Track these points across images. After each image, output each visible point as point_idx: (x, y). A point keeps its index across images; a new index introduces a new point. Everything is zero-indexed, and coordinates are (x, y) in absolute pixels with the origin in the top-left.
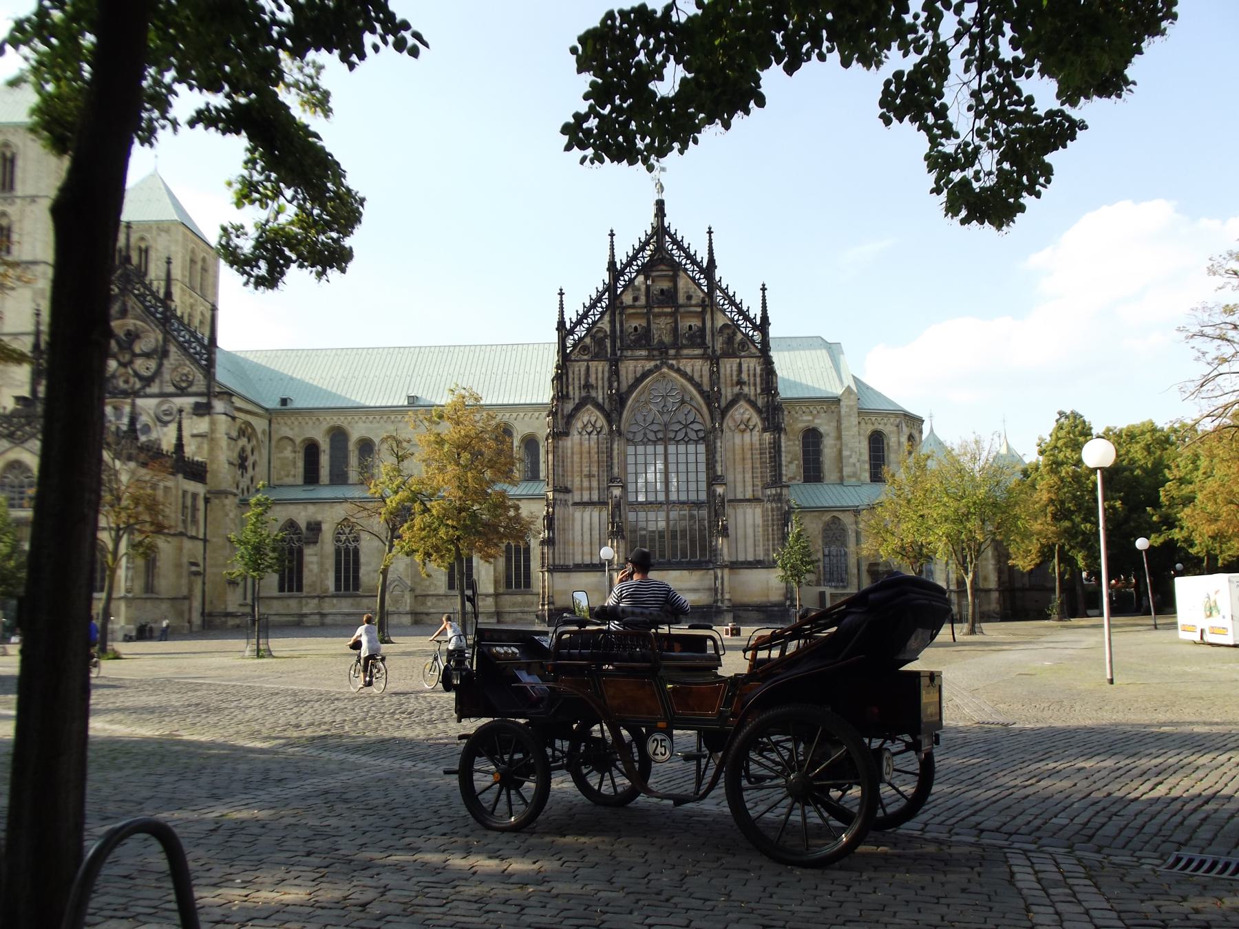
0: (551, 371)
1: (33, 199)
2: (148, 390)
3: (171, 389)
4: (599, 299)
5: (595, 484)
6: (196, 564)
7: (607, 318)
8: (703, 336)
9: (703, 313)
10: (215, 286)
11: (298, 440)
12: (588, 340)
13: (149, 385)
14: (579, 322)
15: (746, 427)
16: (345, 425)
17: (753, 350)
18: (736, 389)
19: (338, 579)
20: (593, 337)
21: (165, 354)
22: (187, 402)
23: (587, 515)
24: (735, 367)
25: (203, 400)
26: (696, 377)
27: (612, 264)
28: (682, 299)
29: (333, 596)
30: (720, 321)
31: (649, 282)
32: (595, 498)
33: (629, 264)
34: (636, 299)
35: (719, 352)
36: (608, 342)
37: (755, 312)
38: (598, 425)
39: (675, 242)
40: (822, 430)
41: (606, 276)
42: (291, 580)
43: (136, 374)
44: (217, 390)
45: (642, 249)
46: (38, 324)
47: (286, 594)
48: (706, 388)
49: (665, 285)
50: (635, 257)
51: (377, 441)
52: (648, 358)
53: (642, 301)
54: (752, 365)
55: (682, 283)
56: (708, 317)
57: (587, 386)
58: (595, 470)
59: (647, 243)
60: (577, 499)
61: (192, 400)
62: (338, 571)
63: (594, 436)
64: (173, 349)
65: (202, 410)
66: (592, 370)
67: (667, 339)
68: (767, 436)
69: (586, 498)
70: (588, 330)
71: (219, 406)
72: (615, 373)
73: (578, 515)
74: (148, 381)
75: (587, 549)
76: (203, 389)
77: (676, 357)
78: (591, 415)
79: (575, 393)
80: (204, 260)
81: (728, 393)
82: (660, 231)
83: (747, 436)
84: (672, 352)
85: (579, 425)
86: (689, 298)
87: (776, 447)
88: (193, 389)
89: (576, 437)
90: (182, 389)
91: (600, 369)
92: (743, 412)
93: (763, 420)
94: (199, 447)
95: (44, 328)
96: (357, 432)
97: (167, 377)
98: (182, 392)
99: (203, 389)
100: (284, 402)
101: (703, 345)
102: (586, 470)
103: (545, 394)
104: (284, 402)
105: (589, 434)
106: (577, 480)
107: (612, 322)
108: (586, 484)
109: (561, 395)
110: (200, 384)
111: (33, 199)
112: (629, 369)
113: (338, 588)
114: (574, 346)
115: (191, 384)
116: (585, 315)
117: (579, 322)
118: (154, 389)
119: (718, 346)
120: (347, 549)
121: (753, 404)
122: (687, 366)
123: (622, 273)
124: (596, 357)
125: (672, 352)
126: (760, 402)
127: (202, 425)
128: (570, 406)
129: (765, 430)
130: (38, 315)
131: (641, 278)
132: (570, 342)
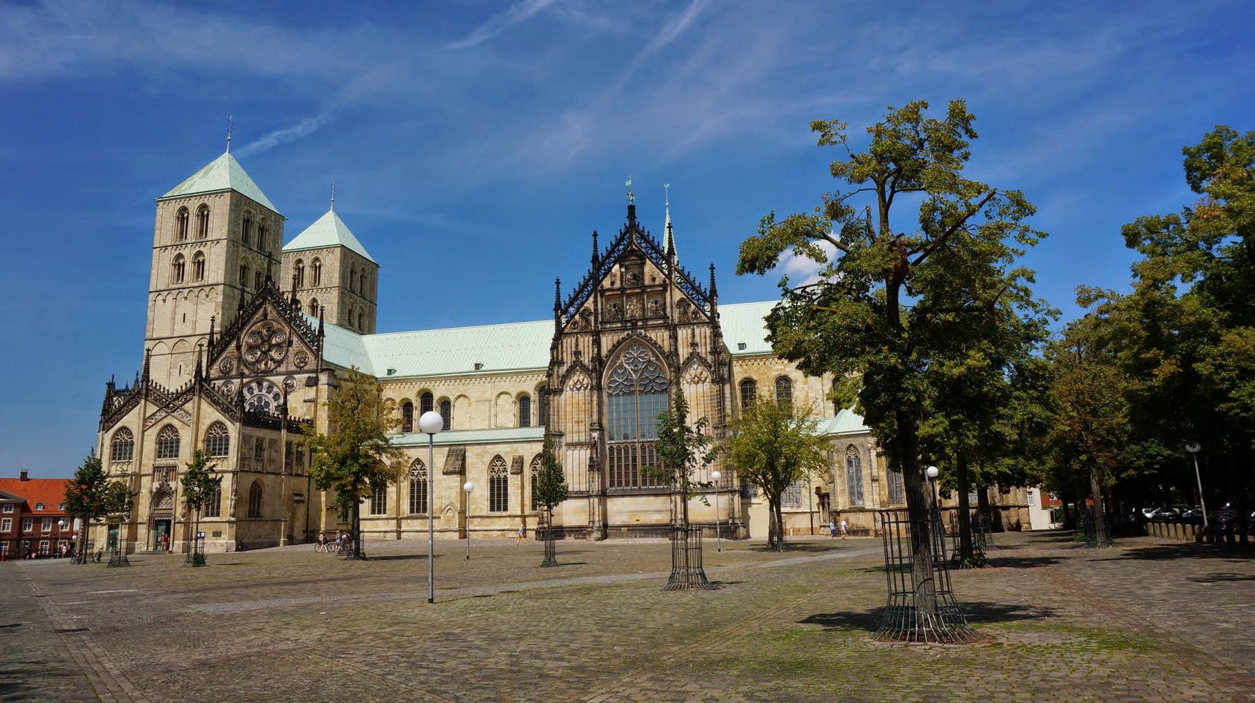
0: (549, 343)
1: (218, 241)
2: (279, 370)
3: (293, 368)
4: (586, 285)
5: (582, 428)
6: (301, 495)
7: (591, 299)
8: (664, 309)
9: (665, 290)
10: (373, 287)
11: (398, 401)
12: (577, 317)
14: (571, 304)
15: (697, 380)
16: (431, 388)
17: (704, 317)
18: (690, 350)
19: (412, 504)
20: (582, 315)
21: (290, 343)
23: (576, 452)
24: (690, 331)
26: (659, 342)
27: (595, 258)
28: (647, 282)
29: (408, 518)
30: (678, 295)
32: (582, 439)
33: (608, 256)
34: (613, 283)
35: (676, 321)
36: (592, 318)
37: (706, 286)
38: (586, 381)
39: (642, 237)
40: (791, 376)
41: (590, 266)
42: (380, 505)
43: (272, 359)
45: (618, 244)
46: (213, 326)
47: (376, 516)
48: (666, 349)
49: (636, 271)
50: (612, 251)
51: (452, 399)
52: (623, 329)
53: (618, 285)
54: (703, 332)
55: (649, 267)
56: (668, 293)
57: (577, 353)
58: (582, 417)
59: (622, 239)
60: (569, 440)
62: (412, 498)
63: (582, 391)
64: (295, 339)
65: (312, 383)
66: (581, 340)
67: (638, 314)
68: (715, 388)
69: (576, 440)
70: (578, 310)
71: (323, 378)
72: (597, 343)
73: (570, 453)
74: (279, 363)
75: (576, 480)
77: (645, 328)
78: (578, 377)
79: (568, 359)
81: (684, 352)
82: (632, 227)
83: (700, 385)
84: (640, 323)
85: (571, 383)
86: (654, 279)
87: (721, 394)
89: (569, 393)
91: (586, 342)
92: (696, 369)
93: (712, 373)
94: (309, 409)
95: (217, 329)
96: (438, 392)
97: (291, 359)
98: (300, 370)
100: (390, 372)
101: (665, 317)
102: (575, 417)
103: (545, 361)
104: (390, 372)
105: (579, 389)
106: (569, 426)
107: (595, 302)
108: (576, 428)
109: (556, 362)
110: (312, 363)
111: (218, 241)
112: (607, 342)
113: (412, 511)
114: (568, 322)
115: (306, 364)
116: (576, 298)
117: (571, 304)
118: (282, 369)
119: (676, 315)
120: (418, 481)
121: (703, 362)
122: (652, 335)
123: (603, 264)
124: (584, 332)
125: (640, 323)
126: (710, 359)
127: (311, 392)
128: (564, 369)
129: (713, 381)
131: (617, 266)
132: (564, 320)
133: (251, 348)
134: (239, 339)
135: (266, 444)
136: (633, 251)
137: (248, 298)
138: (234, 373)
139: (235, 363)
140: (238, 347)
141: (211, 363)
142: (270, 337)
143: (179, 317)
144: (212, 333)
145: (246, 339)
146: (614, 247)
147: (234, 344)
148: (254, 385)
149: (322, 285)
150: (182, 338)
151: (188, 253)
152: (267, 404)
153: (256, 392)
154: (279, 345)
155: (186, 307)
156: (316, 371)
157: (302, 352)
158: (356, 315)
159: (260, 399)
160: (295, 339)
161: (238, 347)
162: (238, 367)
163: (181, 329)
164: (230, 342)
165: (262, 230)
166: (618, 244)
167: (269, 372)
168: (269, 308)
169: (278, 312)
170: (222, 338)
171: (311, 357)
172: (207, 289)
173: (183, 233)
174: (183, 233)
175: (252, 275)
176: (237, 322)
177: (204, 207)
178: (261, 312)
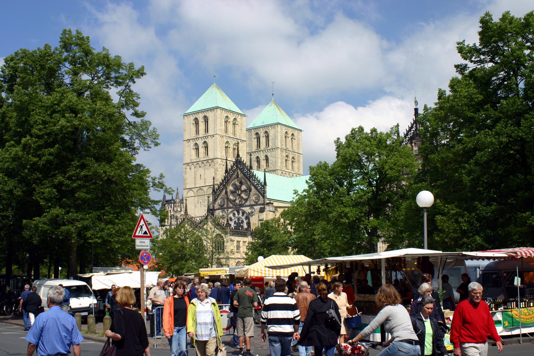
3: (253, 203)
13: (246, 202)
22: (257, 208)
25: (263, 206)
31: (413, 144)
44: (268, 202)
46: (214, 182)
59: (412, 127)
61: (259, 207)
71: (267, 208)
74: (246, 200)
76: (263, 202)
80: (293, 135)
88: (260, 202)
90: (256, 202)
98: (257, 204)
99: (263, 202)
118: (248, 203)
130: (214, 179)
133: (232, 192)
134: (226, 188)
135: (241, 244)
136: (417, 134)
137: (229, 167)
138: (225, 206)
139: (226, 201)
140: (226, 193)
141: (215, 200)
142: (241, 187)
143: (198, 176)
144: (214, 185)
145: (231, 188)
146: (408, 132)
147: (224, 191)
148: (236, 213)
149: (270, 147)
150: (200, 188)
151: (200, 143)
152: (242, 222)
153: (237, 215)
154: (245, 191)
155: (201, 171)
156: (264, 204)
157: (257, 194)
158: (290, 162)
159: (239, 219)
160: (253, 188)
161: (226, 193)
162: (227, 203)
163: (200, 183)
164: (222, 190)
165: (234, 124)
166: (410, 130)
167: (242, 205)
168: (239, 172)
169: (244, 174)
170: (219, 188)
171: (261, 197)
172: (210, 161)
173: (197, 132)
174: (197, 132)
175: (231, 150)
176: (225, 179)
177: (205, 142)
178: (236, 174)
